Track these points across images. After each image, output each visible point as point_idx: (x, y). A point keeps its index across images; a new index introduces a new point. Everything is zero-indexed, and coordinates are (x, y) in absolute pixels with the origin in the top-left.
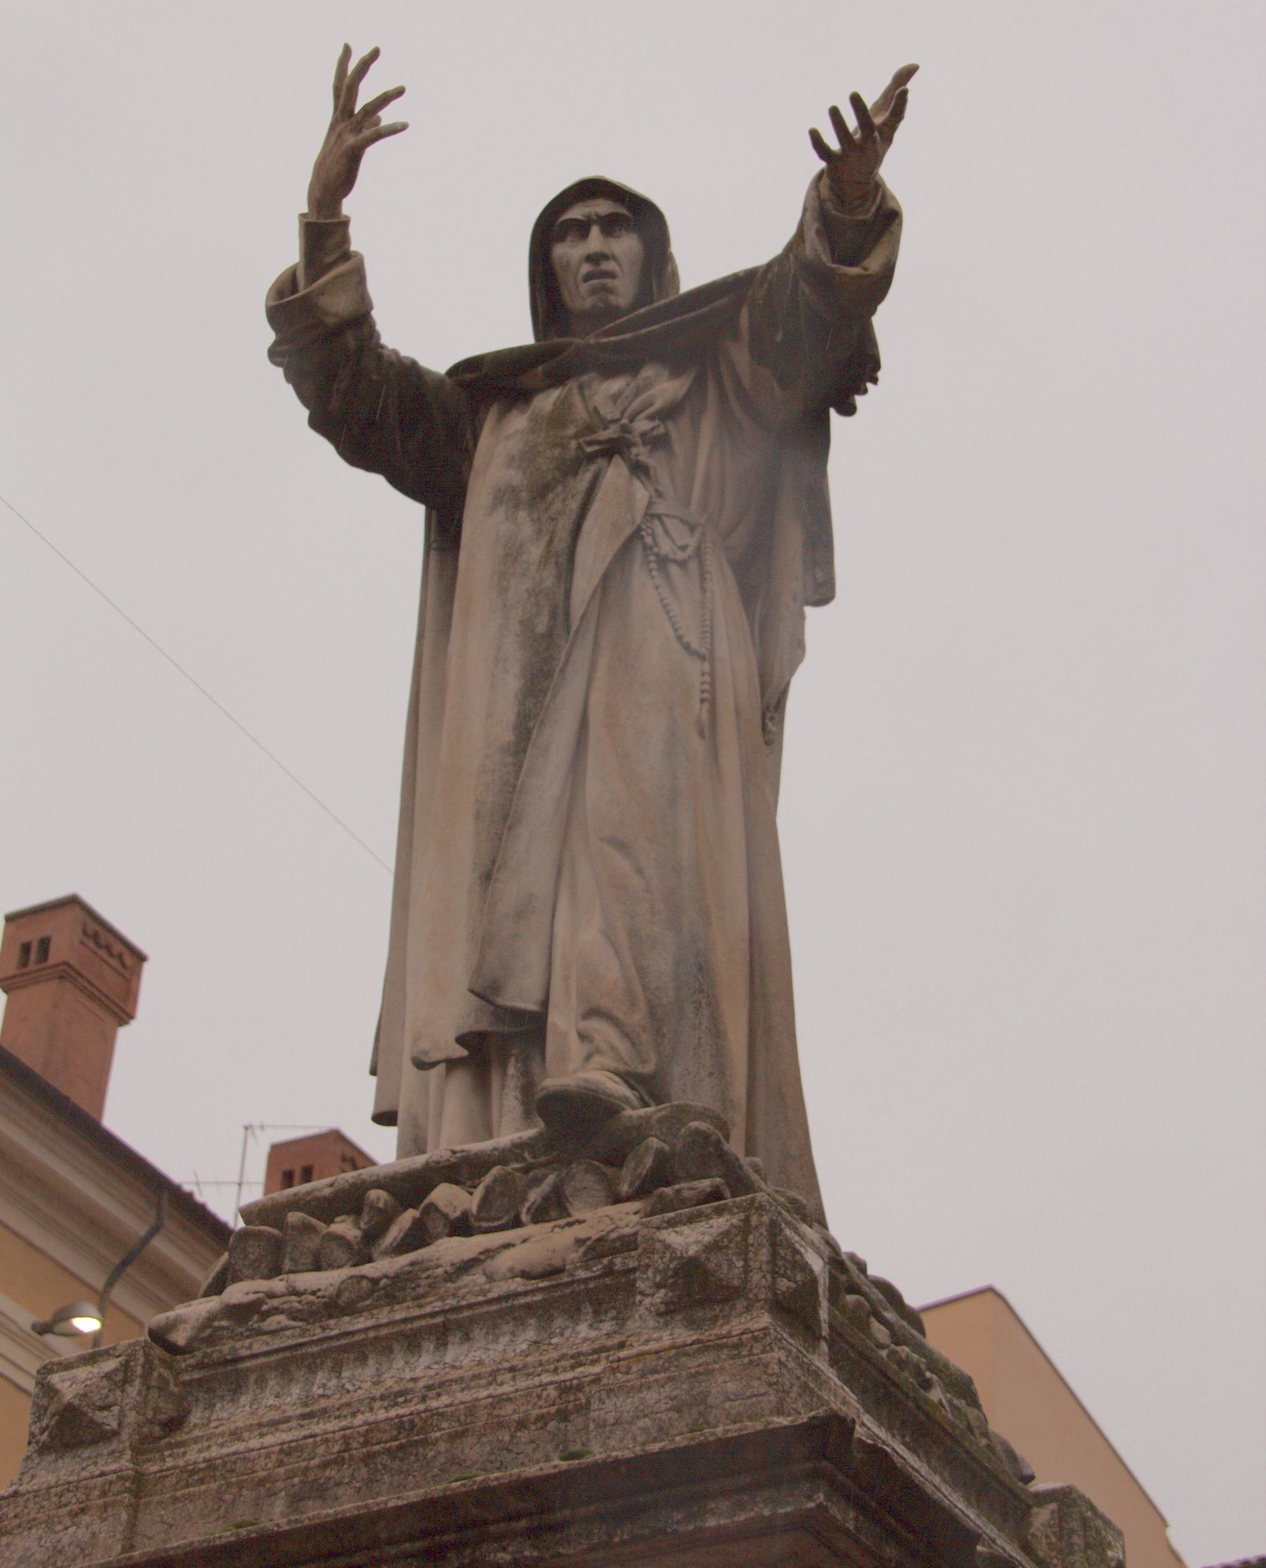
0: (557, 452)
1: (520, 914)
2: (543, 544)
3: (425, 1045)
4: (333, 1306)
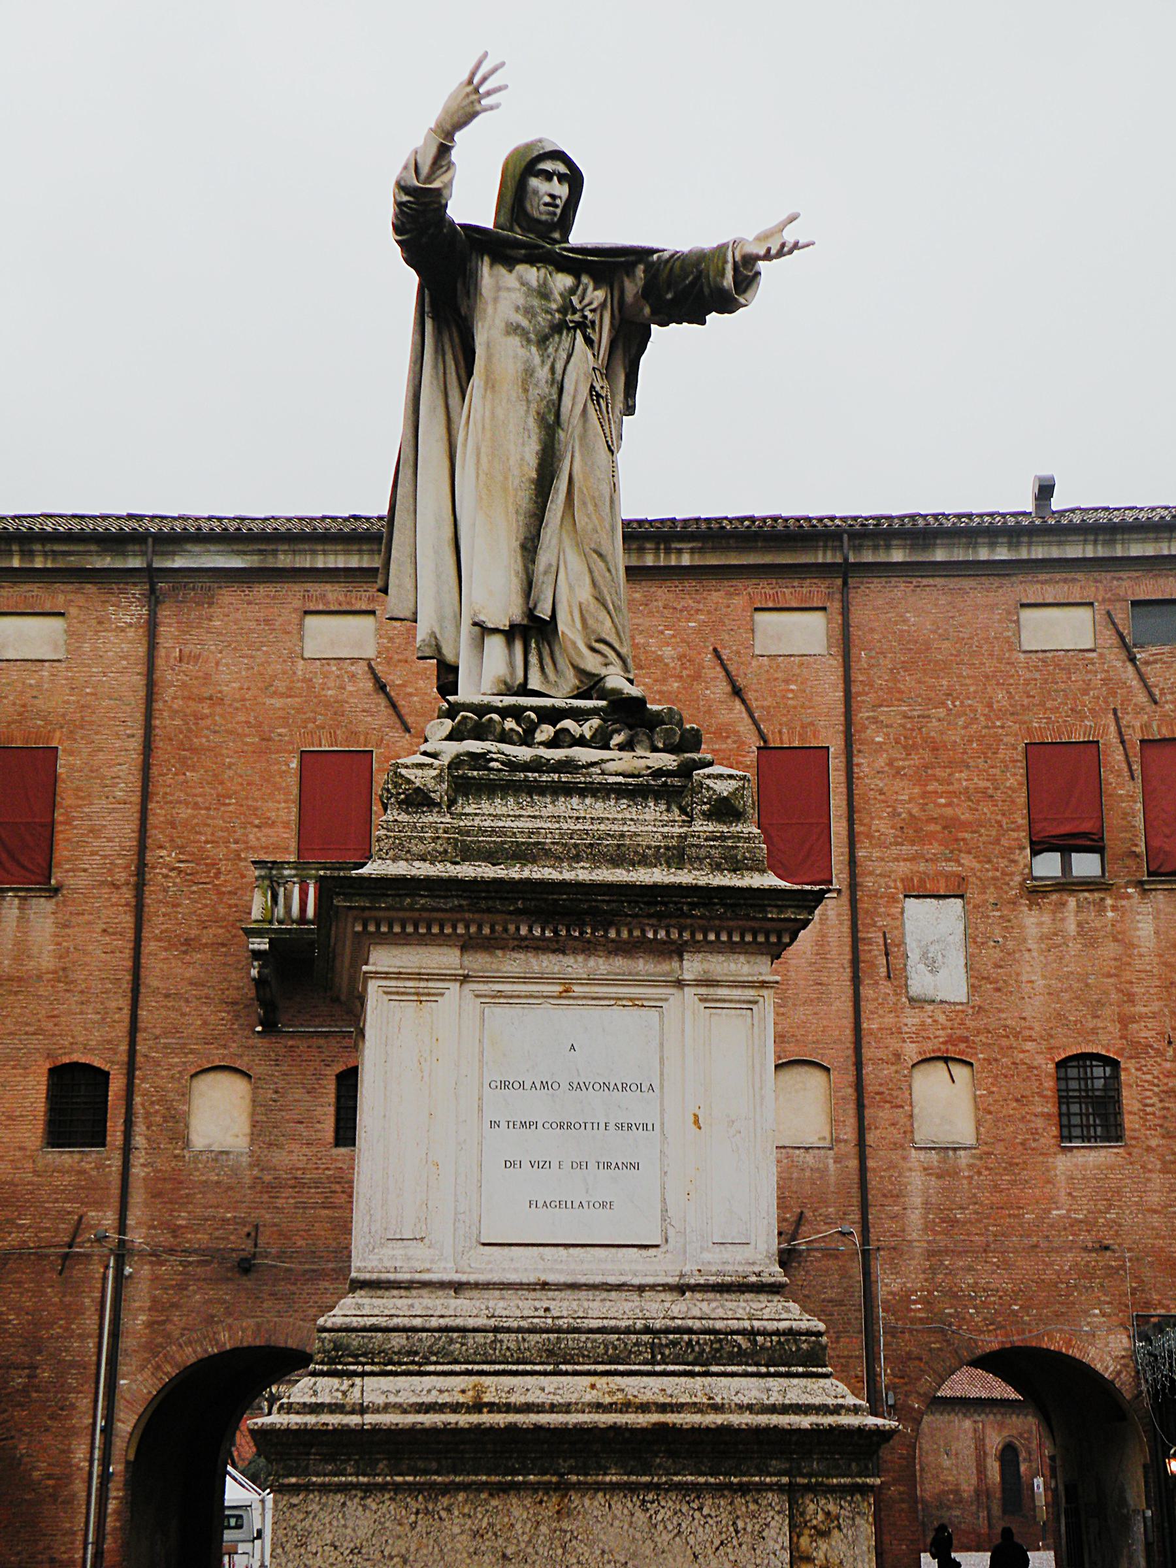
0: (549, 317)
1: (546, 573)
2: (547, 367)
3: (482, 618)
4: (526, 767)
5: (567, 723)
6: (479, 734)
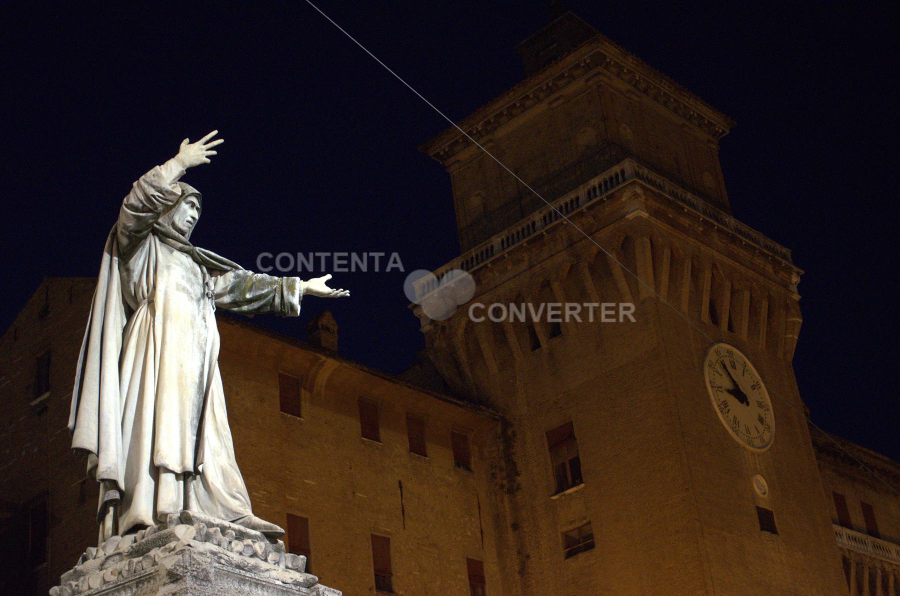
4: (238, 566)
5: (249, 541)
6: (207, 538)
